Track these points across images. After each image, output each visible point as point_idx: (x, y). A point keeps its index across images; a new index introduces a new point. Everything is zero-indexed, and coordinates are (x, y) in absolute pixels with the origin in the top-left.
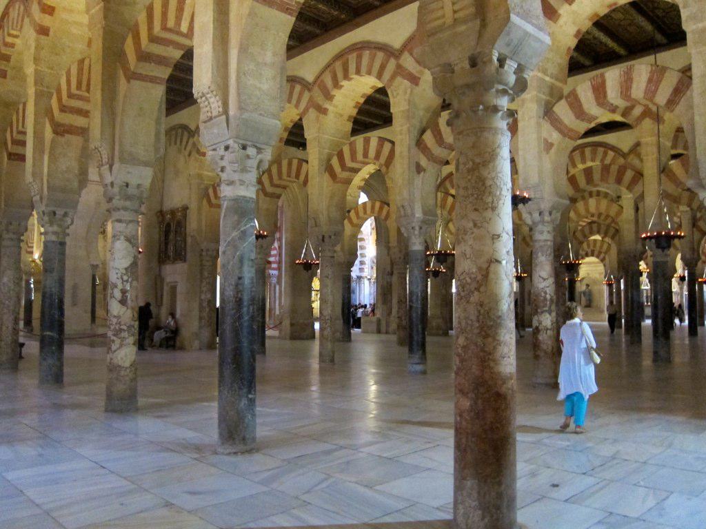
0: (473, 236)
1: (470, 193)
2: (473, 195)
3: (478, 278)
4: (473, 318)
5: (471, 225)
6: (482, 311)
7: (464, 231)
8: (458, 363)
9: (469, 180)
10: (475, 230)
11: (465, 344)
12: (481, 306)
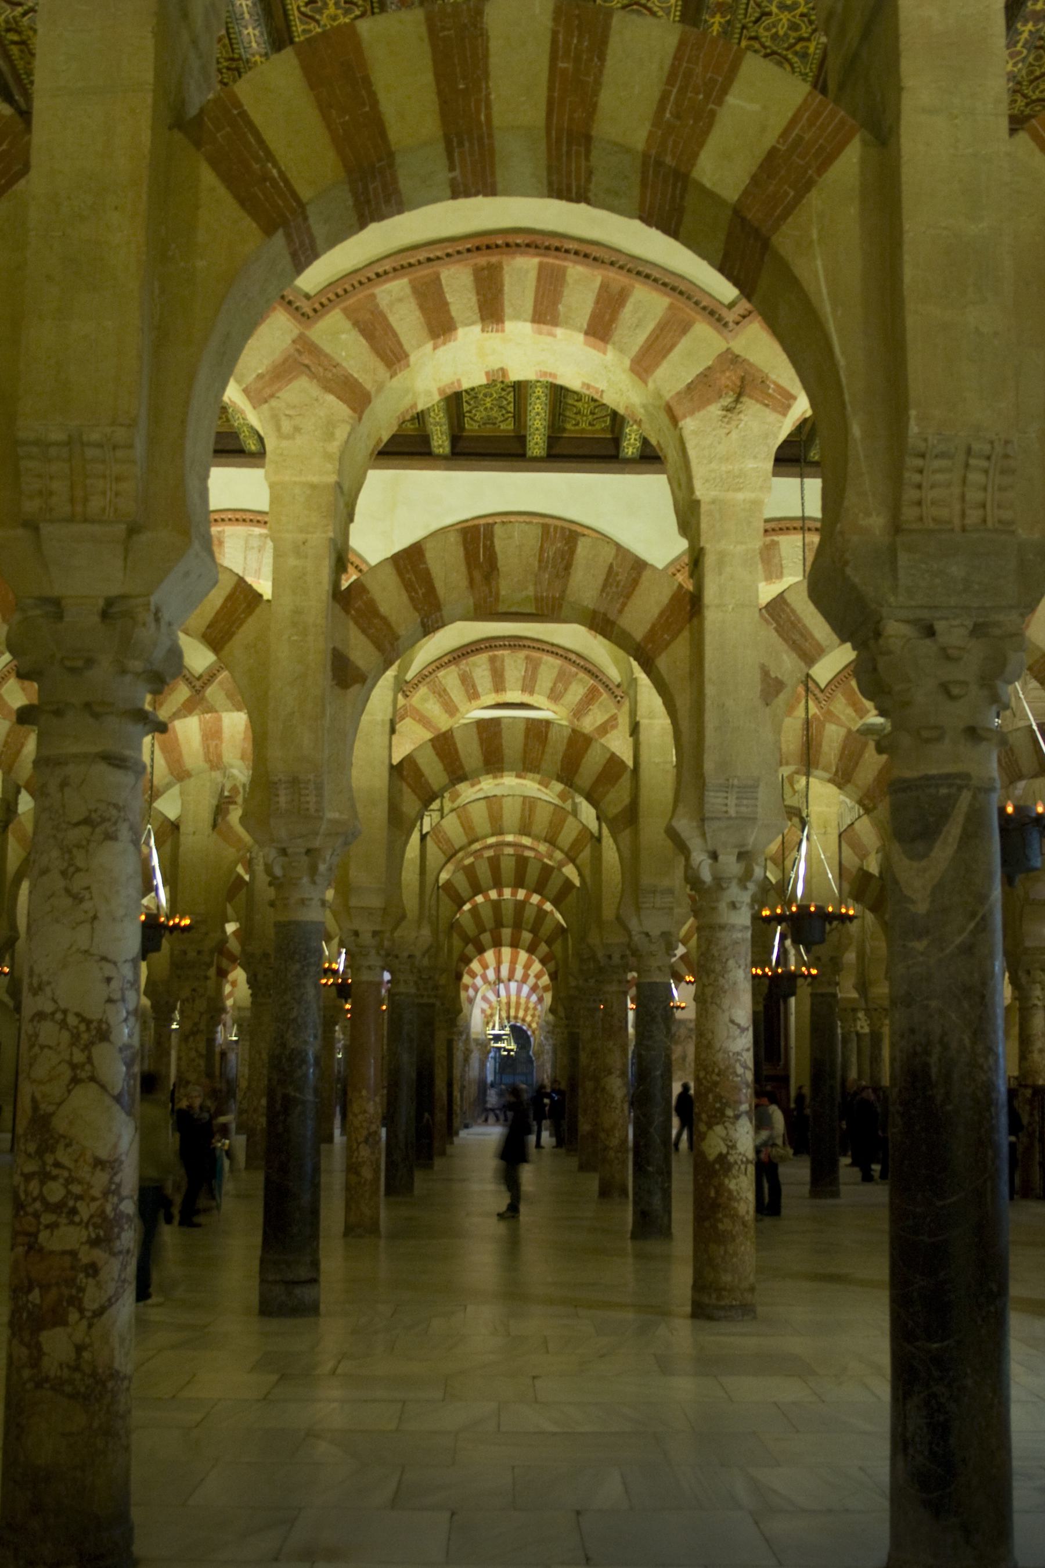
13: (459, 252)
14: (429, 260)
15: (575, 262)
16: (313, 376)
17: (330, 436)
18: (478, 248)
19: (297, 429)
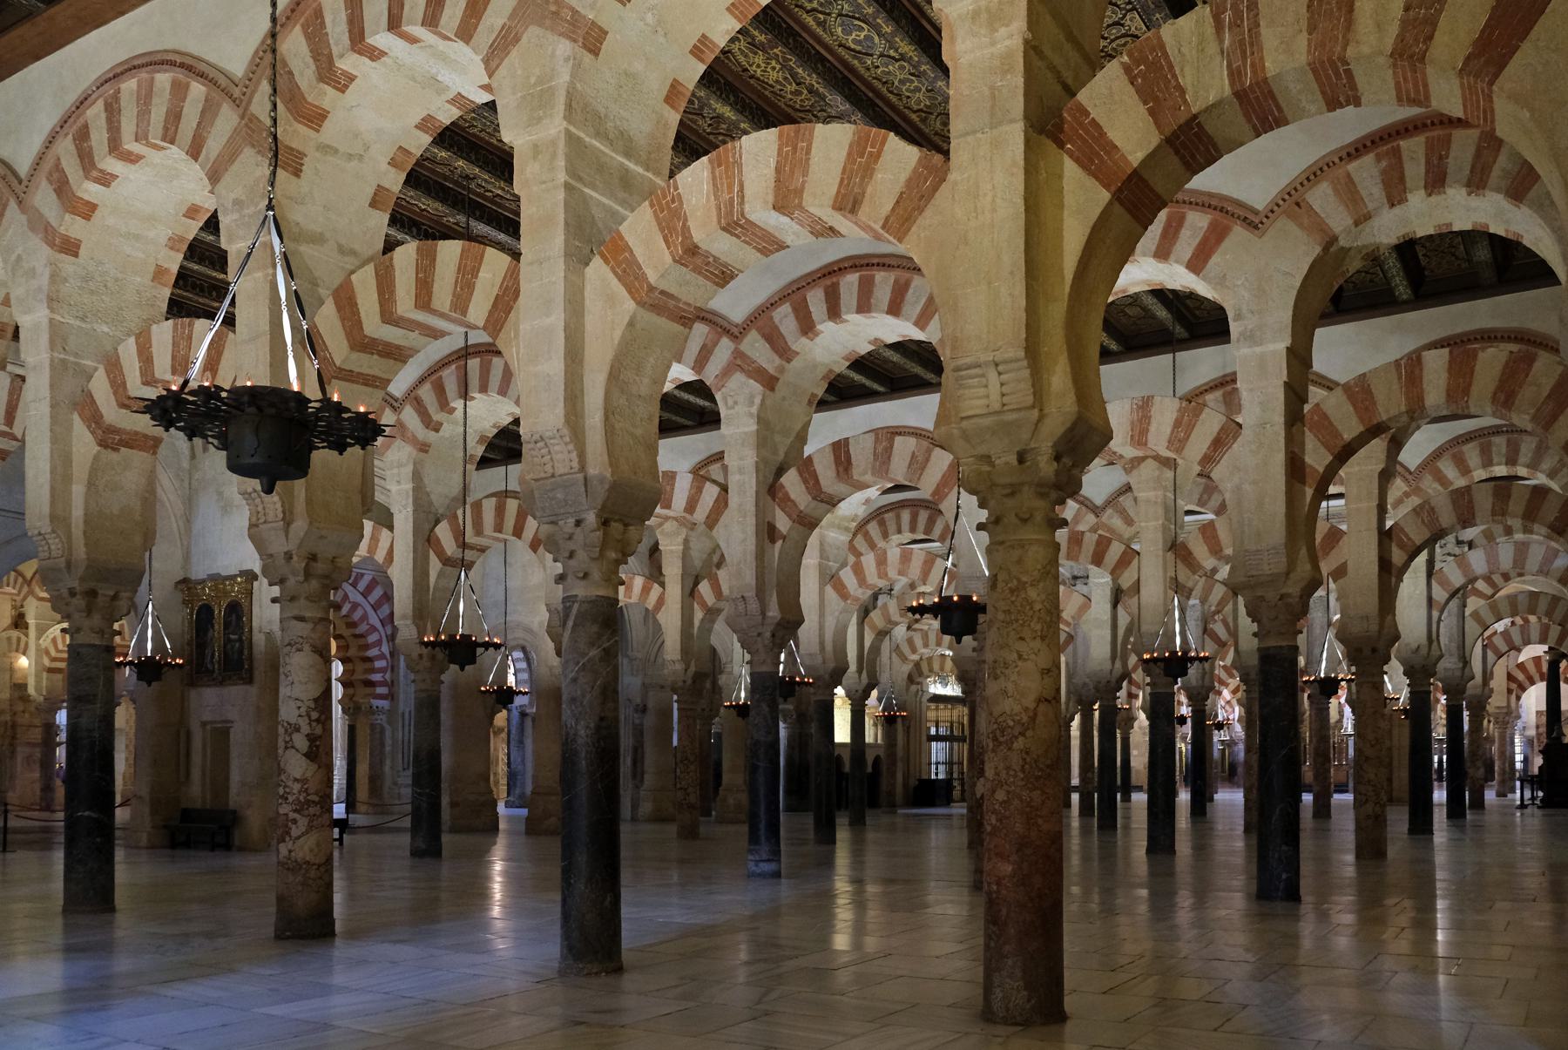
0: (1017, 670)
2: (1017, 621)
4: (1017, 768)
5: (1015, 655)
6: (1028, 760)
7: (1005, 663)
8: (994, 822)
10: (1020, 663)
12: (1027, 753)
13: (814, 281)
14: (798, 289)
15: (880, 270)
16: (743, 370)
17: (751, 403)
18: (824, 275)
19: (736, 403)
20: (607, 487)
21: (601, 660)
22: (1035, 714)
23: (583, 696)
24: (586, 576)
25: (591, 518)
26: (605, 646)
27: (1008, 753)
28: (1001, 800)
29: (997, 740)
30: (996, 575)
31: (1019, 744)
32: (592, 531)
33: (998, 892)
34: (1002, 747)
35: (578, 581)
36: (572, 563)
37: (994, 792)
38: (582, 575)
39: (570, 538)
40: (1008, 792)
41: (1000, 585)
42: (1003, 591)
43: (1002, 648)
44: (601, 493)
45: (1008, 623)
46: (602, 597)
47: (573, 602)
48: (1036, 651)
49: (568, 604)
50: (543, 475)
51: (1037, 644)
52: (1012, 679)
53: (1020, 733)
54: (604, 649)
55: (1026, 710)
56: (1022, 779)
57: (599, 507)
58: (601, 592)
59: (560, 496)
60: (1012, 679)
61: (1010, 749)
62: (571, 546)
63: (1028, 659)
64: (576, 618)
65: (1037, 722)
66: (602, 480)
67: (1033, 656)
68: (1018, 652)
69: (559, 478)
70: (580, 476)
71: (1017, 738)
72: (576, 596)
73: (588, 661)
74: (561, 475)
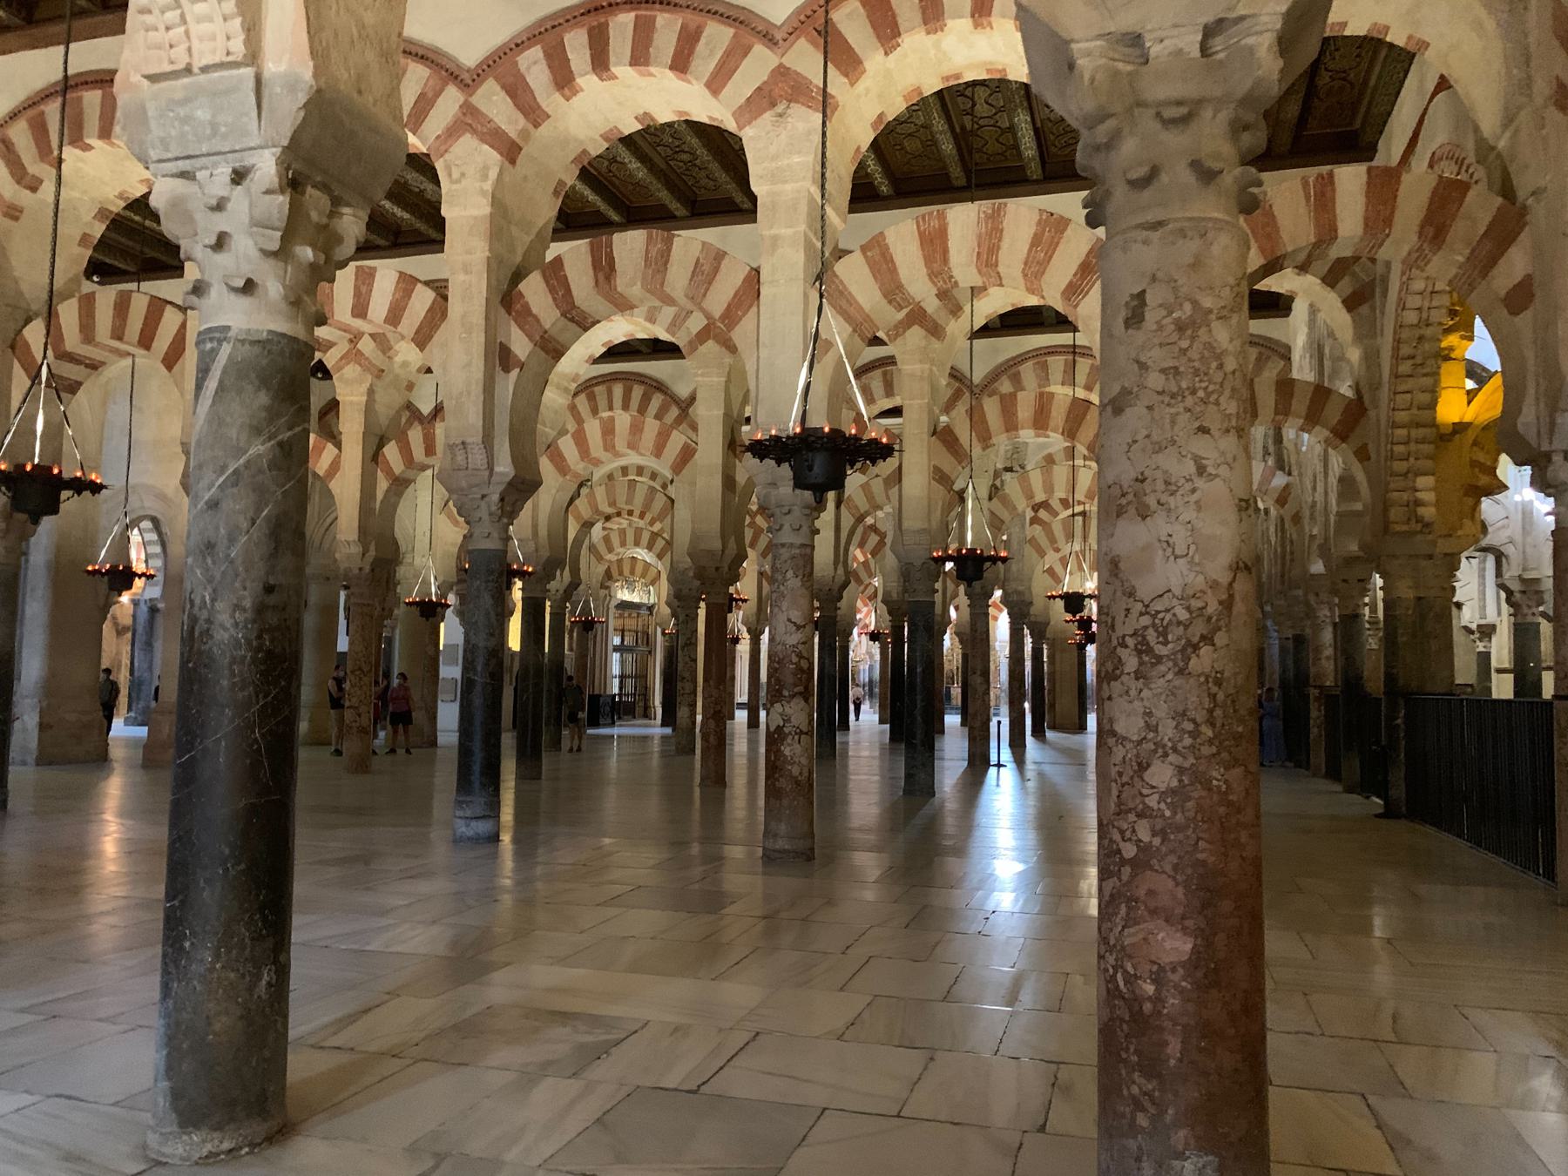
1: (1184, 385)
2: (1194, 392)
3: (1210, 610)
4: (1200, 716)
5: (1190, 468)
6: (1221, 696)
7: (1167, 483)
9: (1184, 351)
11: (1175, 783)
12: (1218, 683)
20: (302, 98)
21: (273, 465)
22: (1231, 596)
23: (232, 540)
24: (249, 287)
25: (266, 166)
26: (285, 435)
27: (1177, 682)
28: (1163, 787)
29: (1150, 650)
30: (1141, 295)
31: (1204, 660)
32: (268, 192)
33: (1158, 999)
34: (1163, 668)
35: (233, 296)
36: (221, 259)
37: (1143, 767)
38: (240, 283)
39: (219, 206)
40: (1181, 770)
41: (1152, 316)
42: (1160, 328)
43: (1159, 449)
44: (287, 111)
45: (1173, 396)
46: (283, 335)
47: (220, 341)
48: (1230, 461)
49: (209, 346)
50: (168, 68)
51: (1229, 443)
52: (1185, 517)
53: (1203, 638)
54: (281, 444)
55: (1214, 585)
56: (1210, 742)
57: (285, 143)
58: (282, 326)
59: (202, 114)
60: (1185, 517)
61: (1181, 672)
62: (221, 222)
63: (1217, 476)
64: (224, 372)
65: (1234, 613)
66: (292, 85)
67: (1223, 471)
68: (1197, 459)
69: (202, 78)
70: (248, 72)
71: (1196, 647)
72: (228, 328)
73: (247, 465)
74: (205, 69)
